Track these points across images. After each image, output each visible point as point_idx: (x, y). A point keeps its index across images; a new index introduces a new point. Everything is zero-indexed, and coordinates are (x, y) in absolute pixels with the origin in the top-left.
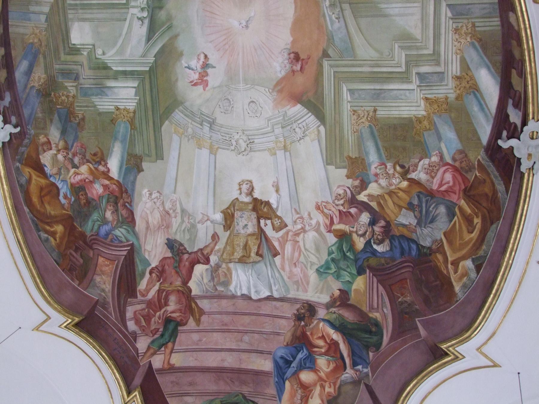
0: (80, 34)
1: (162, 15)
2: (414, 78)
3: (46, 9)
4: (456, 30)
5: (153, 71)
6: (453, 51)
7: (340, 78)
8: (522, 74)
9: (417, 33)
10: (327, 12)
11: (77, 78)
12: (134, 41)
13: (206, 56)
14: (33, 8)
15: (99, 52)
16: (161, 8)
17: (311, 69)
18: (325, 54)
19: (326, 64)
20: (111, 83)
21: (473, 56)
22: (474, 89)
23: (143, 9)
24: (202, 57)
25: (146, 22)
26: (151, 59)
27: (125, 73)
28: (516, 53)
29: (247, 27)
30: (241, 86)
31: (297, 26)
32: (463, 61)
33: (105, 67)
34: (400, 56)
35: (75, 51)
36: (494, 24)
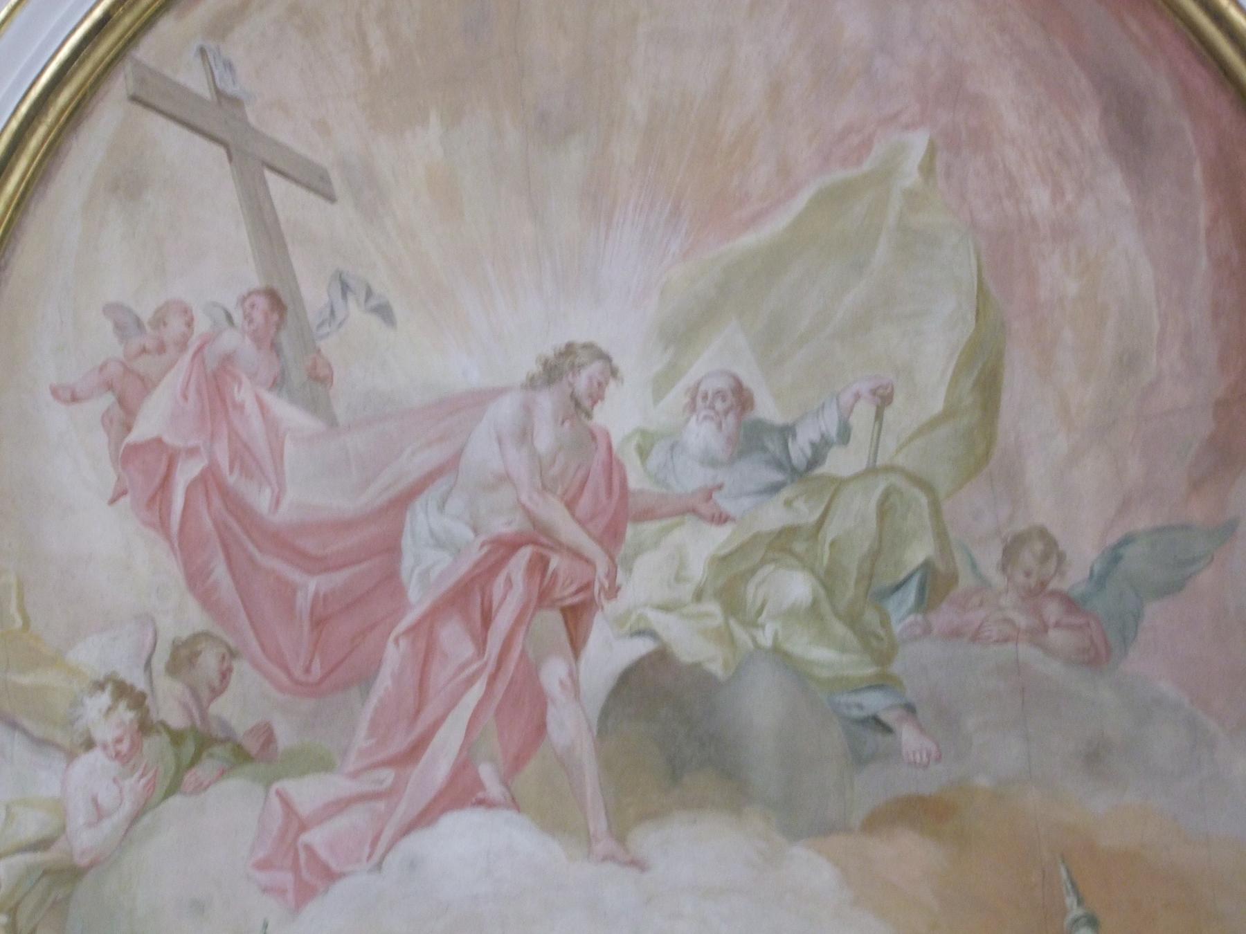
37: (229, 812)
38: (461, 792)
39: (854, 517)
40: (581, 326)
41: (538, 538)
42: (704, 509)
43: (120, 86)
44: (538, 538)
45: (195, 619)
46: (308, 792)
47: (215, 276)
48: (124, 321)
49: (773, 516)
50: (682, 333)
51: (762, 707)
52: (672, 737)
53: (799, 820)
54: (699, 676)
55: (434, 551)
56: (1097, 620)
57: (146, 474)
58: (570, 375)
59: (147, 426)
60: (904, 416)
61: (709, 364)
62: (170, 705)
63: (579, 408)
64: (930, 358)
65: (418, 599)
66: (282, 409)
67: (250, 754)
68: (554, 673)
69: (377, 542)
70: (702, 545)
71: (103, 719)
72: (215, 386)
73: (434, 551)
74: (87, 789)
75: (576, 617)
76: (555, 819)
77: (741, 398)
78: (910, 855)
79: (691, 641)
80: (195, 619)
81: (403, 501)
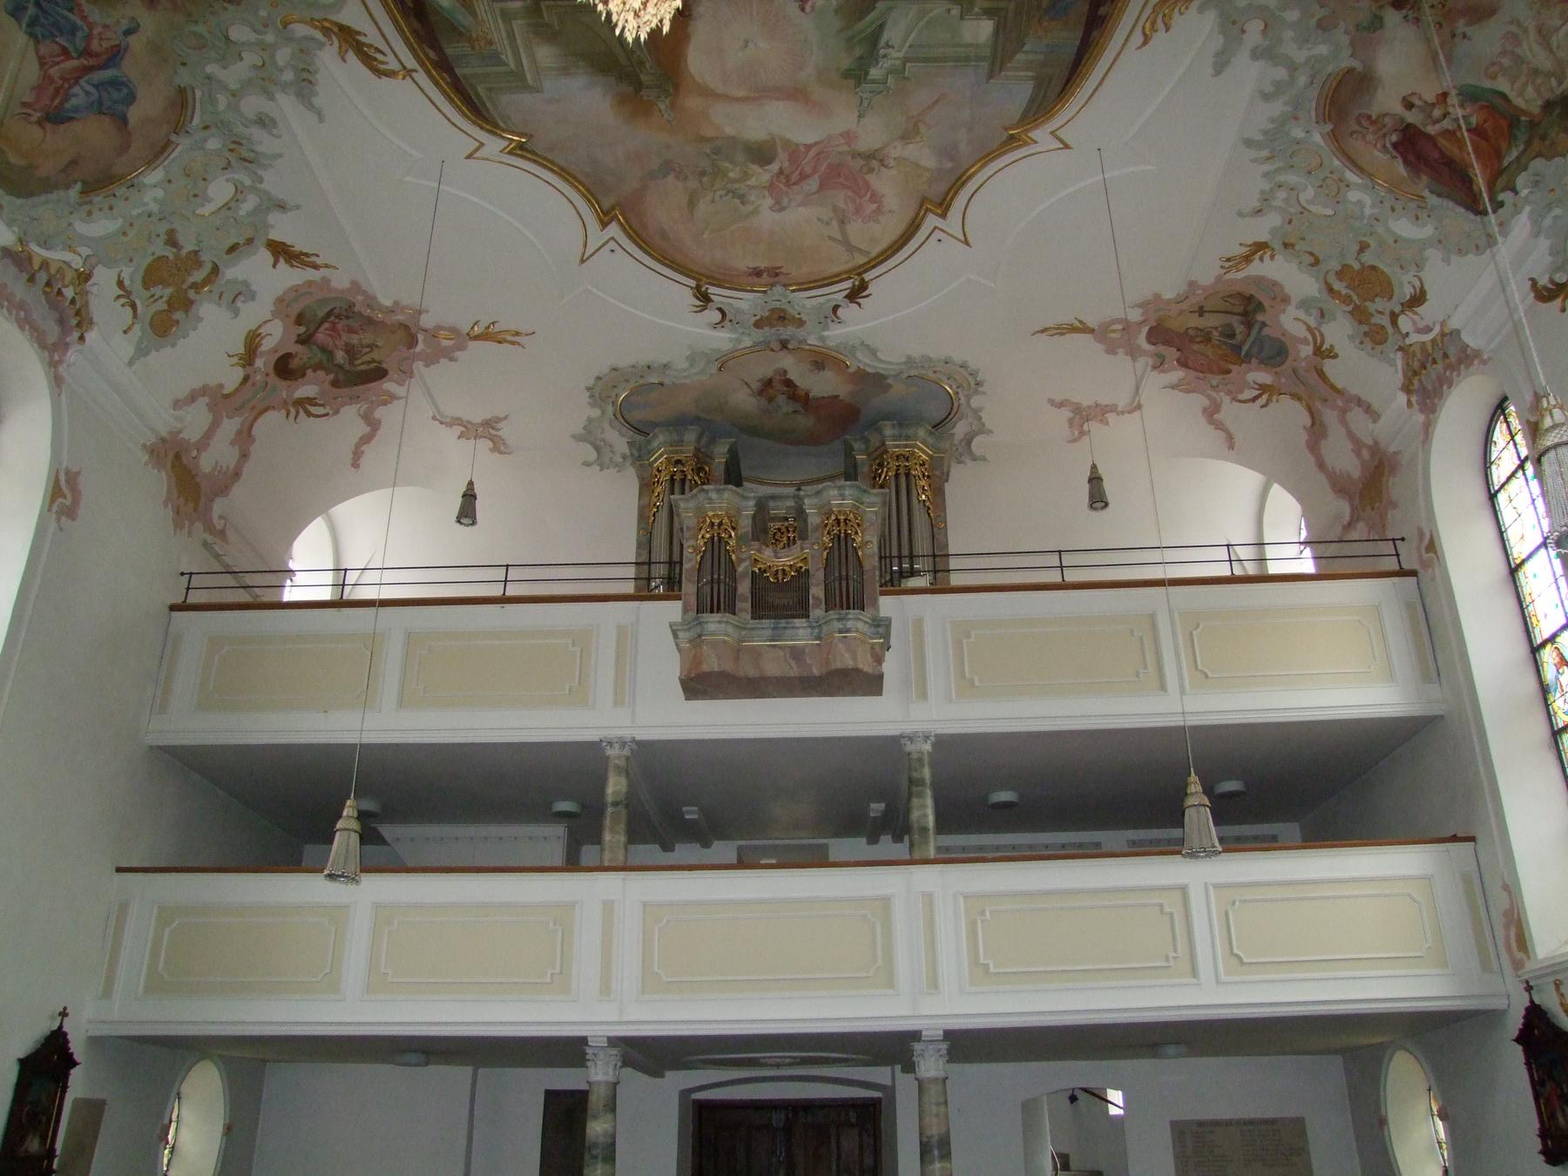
0: (981, 30)
1: (858, 52)
3: (1019, 56)
4: (491, 43)
13: (803, 10)
14: (1041, 57)
15: (956, 11)
16: (861, 58)
21: (463, 18)
23: (885, 56)
24: (808, 8)
25: (882, 43)
28: (416, 25)
29: (747, 42)
32: (474, 14)
35: (989, 13)
37: (865, 143)
38: (808, 147)
40: (777, 216)
41: (788, 183)
42: (751, 187)
43: (873, 254)
44: (788, 183)
45: (867, 177)
46: (845, 148)
47: (855, 230)
48: (878, 222)
49: (736, 186)
50: (756, 212)
52: (761, 154)
53: (733, 141)
54: (753, 162)
55: (813, 184)
56: (667, 168)
57: (875, 198)
58: (779, 207)
59: (874, 206)
60: (708, 198)
61: (750, 208)
62: (875, 163)
63: (778, 203)
64: (703, 206)
65: (816, 176)
66: (842, 205)
67: (856, 155)
68: (786, 164)
69: (823, 186)
70: (753, 182)
71: (892, 163)
73: (813, 184)
74: (896, 151)
75: (781, 172)
76: (787, 143)
77: (743, 203)
79: (755, 168)
80: (867, 177)
81: (818, 192)
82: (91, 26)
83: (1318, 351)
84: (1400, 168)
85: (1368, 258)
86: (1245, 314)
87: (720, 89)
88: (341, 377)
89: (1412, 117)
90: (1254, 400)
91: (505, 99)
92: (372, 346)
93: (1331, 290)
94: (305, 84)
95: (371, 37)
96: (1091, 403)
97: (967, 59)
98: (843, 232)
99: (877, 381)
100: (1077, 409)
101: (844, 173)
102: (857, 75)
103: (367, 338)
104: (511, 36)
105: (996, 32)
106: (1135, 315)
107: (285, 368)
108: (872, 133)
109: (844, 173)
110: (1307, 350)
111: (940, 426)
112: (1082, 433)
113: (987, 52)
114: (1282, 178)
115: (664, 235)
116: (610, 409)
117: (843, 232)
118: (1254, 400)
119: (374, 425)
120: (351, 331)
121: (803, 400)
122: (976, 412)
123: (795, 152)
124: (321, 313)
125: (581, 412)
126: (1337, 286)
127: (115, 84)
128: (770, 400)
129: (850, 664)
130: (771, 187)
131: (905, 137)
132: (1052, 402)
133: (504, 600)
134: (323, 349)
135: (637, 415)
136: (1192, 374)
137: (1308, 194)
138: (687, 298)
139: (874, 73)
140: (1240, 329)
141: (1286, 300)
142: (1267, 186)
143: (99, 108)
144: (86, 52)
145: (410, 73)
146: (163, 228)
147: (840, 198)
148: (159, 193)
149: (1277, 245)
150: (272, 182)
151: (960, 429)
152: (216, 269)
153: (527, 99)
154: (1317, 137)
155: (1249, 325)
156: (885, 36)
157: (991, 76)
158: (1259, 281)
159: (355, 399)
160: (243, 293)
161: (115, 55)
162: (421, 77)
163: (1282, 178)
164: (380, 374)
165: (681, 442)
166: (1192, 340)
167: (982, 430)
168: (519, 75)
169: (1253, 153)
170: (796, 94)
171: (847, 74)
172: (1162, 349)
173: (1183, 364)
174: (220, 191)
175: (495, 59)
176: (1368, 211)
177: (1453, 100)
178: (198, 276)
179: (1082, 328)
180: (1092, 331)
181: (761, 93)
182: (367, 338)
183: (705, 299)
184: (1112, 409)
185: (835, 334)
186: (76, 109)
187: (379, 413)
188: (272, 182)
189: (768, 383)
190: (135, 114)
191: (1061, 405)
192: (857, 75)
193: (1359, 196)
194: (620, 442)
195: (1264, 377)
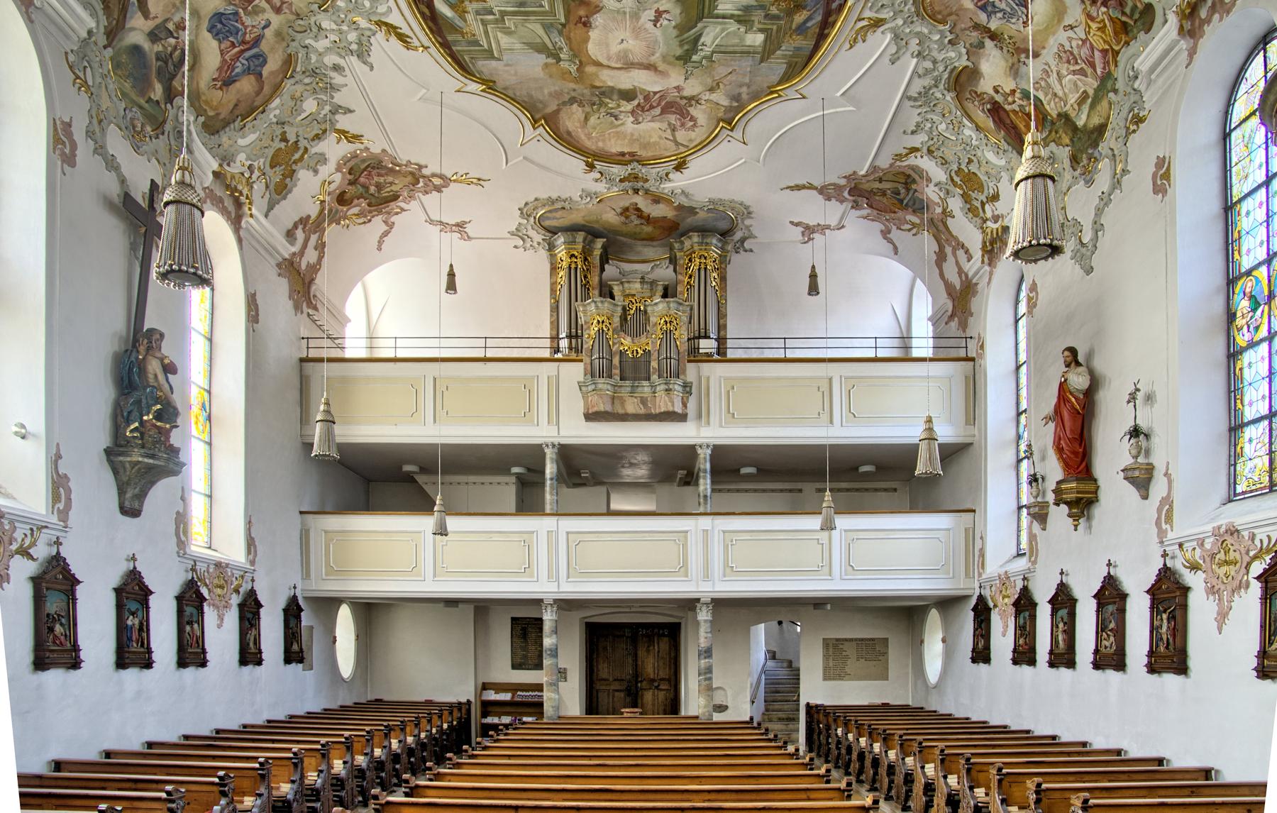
0: (757, 39)
1: (686, 47)
2: (496, 10)
5: (700, 19)
6: (473, 25)
7: (552, 12)
8: (422, 14)
9: (499, 35)
10: (564, 45)
11: (766, 16)
12: (712, 35)
15: (743, 29)
17: (573, 19)
18: (564, 25)
19: (563, 20)
20: (736, 12)
21: (459, 22)
22: (452, 6)
26: (700, 25)
27: (724, 17)
28: (431, 24)
30: (628, 10)
31: (587, 40)
32: (465, 21)
33: (739, 22)
34: (509, 22)
35: (761, 30)
36: (450, 38)
37: (686, 93)
38: (655, 93)
39: (602, 110)
51: (615, 97)
52: (628, 95)
53: (612, 89)
55: (658, 111)
56: (573, 100)
57: (693, 119)
64: (593, 120)
69: (663, 112)
72: (683, 125)
73: (658, 111)
75: (639, 105)
76: (643, 91)
78: (597, 84)
82: (246, 28)
83: (944, 211)
84: (991, 124)
85: (973, 168)
86: (906, 183)
87: (605, 62)
88: (373, 201)
89: (998, 98)
90: (909, 230)
91: (480, 63)
92: (391, 183)
93: (952, 180)
94: (362, 53)
95: (405, 30)
96: (815, 223)
97: (749, 53)
98: (674, 136)
99: (692, 211)
100: (807, 227)
101: (676, 107)
102: (685, 58)
103: (390, 179)
104: (486, 33)
105: (766, 41)
106: (843, 182)
107: (342, 199)
108: (692, 88)
109: (676, 107)
110: (939, 210)
111: (725, 234)
112: (810, 239)
113: (760, 49)
114: (929, 116)
115: (569, 133)
116: (532, 219)
117: (674, 136)
118: (909, 230)
119: (391, 226)
120: (379, 175)
121: (648, 219)
122: (748, 228)
123: (647, 97)
124: (363, 167)
125: (515, 220)
126: (957, 179)
127: (256, 56)
128: (627, 217)
129: (671, 409)
130: (633, 112)
131: (711, 90)
132: (792, 223)
133: (485, 360)
134: (364, 186)
135: (547, 223)
136: (875, 212)
137: (942, 127)
138: (583, 165)
139: (695, 58)
140: (903, 191)
141: (929, 180)
142: (919, 119)
143: (248, 71)
144: (243, 42)
145: (426, 48)
146: (279, 131)
147: (673, 118)
148: (277, 112)
149: (925, 150)
150: (339, 98)
151: (738, 235)
152: (306, 149)
153: (494, 63)
154: (948, 98)
155: (908, 190)
156: (702, 40)
157: (762, 61)
158: (915, 169)
159: (380, 212)
160: (322, 159)
161: (257, 41)
162: (433, 50)
163: (929, 116)
164: (395, 197)
165: (574, 242)
166: (875, 194)
167: (752, 236)
168: (490, 51)
169: (912, 103)
170: (650, 67)
171: (678, 58)
172: (860, 199)
173: (871, 206)
174: (310, 106)
175: (476, 43)
176: (974, 142)
177: (1018, 95)
178: (297, 156)
179: (811, 187)
180: (816, 188)
181: (629, 65)
182: (390, 179)
183: (591, 167)
184: (828, 227)
185: (667, 186)
186: (237, 75)
187: (394, 219)
188: (339, 98)
189: (627, 209)
190: (265, 72)
191: (797, 225)
192: (685, 58)
193: (969, 132)
194: (538, 237)
195: (916, 220)
